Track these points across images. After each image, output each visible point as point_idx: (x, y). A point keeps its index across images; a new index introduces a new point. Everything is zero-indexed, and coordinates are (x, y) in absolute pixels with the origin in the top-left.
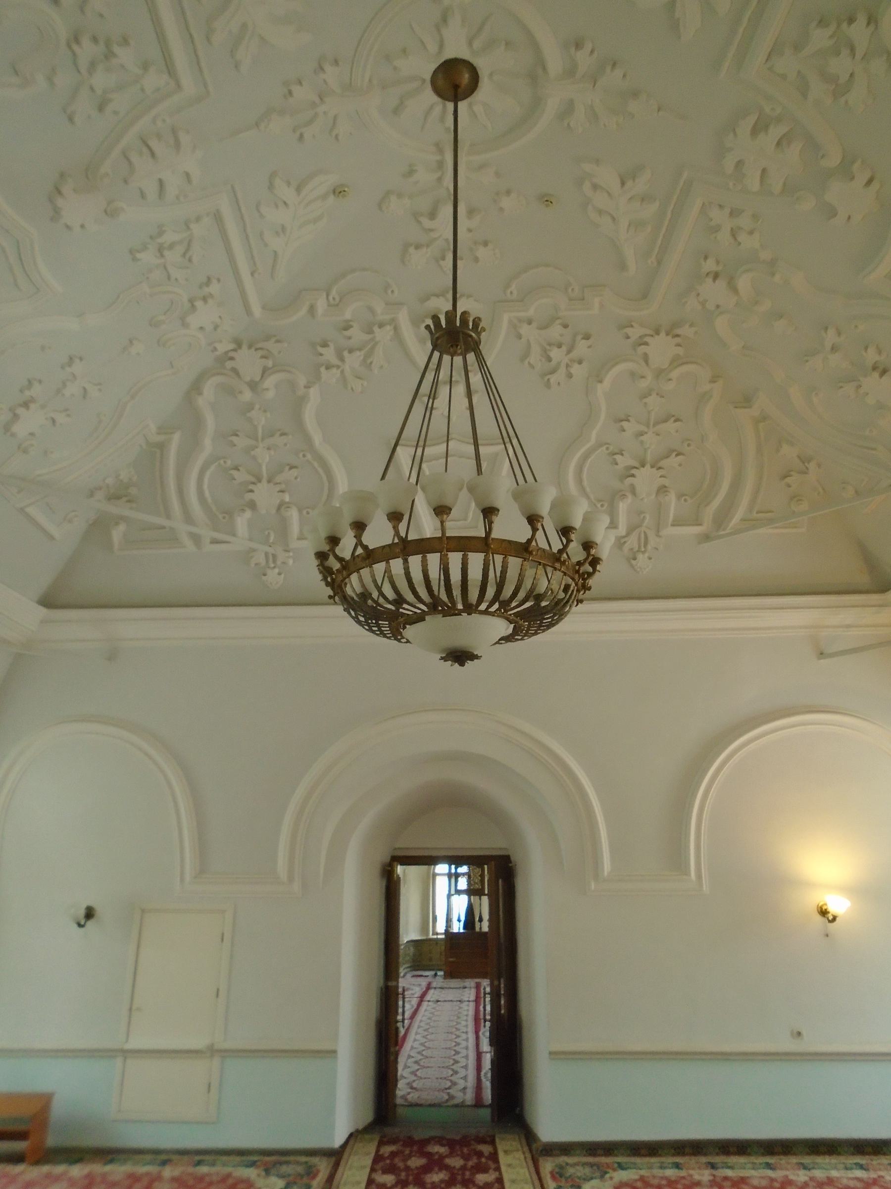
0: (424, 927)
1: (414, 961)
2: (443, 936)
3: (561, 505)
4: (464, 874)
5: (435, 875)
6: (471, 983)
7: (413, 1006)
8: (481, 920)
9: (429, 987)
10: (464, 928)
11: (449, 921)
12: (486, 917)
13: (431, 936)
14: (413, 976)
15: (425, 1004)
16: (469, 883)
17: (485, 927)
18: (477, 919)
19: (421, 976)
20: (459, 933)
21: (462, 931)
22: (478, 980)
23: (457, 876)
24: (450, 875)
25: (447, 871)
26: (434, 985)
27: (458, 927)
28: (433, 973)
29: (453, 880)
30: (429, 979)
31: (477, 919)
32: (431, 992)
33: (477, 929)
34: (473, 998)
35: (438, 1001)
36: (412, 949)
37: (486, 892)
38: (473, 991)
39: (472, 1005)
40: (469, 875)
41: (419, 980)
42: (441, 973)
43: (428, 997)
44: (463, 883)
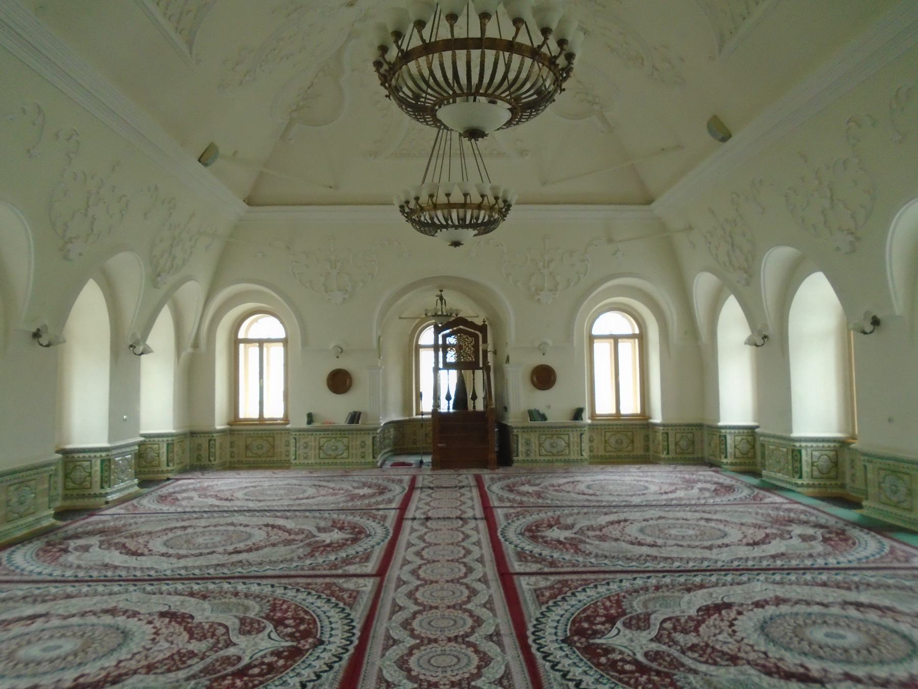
0: (407, 405)
1: (395, 444)
2: (430, 416)
3: (539, 11)
4: (451, 346)
5: (418, 347)
6: (467, 476)
7: (387, 534)
8: (474, 397)
9: (412, 487)
10: (454, 408)
11: (436, 398)
12: (480, 394)
13: (414, 416)
14: (396, 465)
15: (407, 525)
16: (458, 357)
17: (480, 406)
18: (469, 396)
19: (403, 464)
20: (448, 413)
21: (451, 410)
22: (476, 471)
23: (446, 347)
24: (436, 347)
25: (432, 342)
26: (419, 484)
27: (445, 407)
28: (418, 458)
29: (441, 354)
30: (413, 471)
31: (469, 396)
32: (417, 495)
33: (470, 408)
34: (479, 512)
35: (428, 519)
36: (392, 430)
37: (481, 365)
38: (475, 493)
39: (482, 525)
40: (459, 348)
41: (402, 470)
42: (427, 459)
43: (410, 514)
44: (451, 357)
